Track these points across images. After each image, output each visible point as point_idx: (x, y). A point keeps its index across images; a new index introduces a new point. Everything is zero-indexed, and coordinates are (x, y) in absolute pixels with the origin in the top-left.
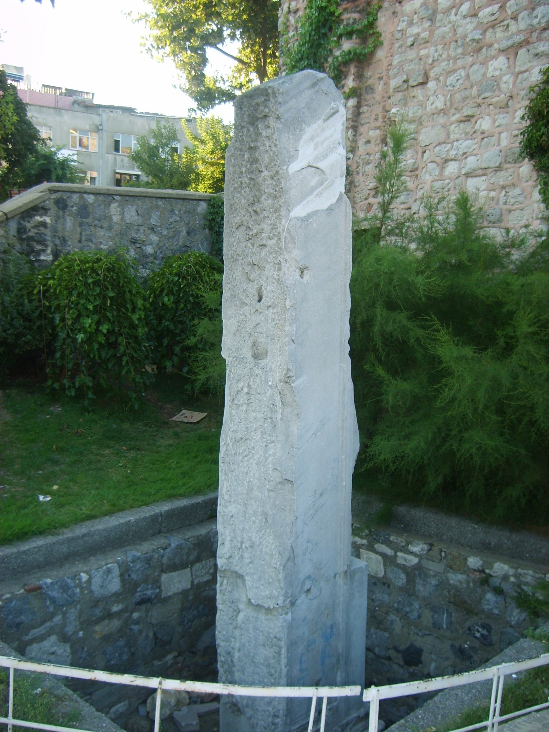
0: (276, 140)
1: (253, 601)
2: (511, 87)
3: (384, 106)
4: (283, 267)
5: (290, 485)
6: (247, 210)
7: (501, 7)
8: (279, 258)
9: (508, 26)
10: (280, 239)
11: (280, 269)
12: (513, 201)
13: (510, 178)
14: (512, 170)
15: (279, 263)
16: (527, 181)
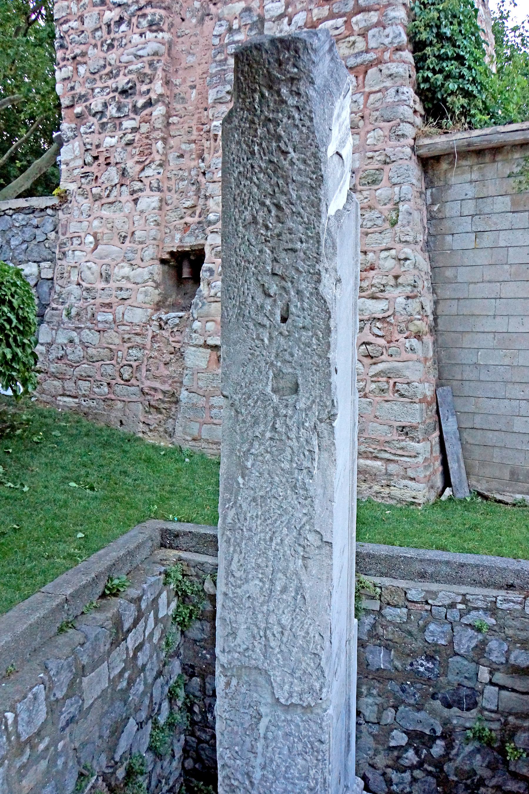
0: (311, 112)
1: (282, 701)
2: (362, 107)
3: (200, 118)
4: (323, 277)
5: (328, 548)
6: (263, 204)
7: (345, 22)
8: (317, 266)
9: (354, 43)
10: (319, 242)
11: (319, 281)
12: (369, 224)
13: (366, 200)
14: (368, 192)
15: (319, 274)
16: (385, 204)
